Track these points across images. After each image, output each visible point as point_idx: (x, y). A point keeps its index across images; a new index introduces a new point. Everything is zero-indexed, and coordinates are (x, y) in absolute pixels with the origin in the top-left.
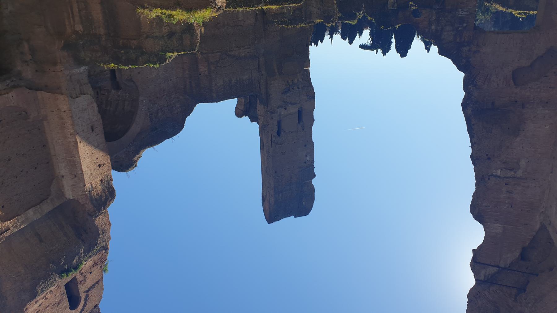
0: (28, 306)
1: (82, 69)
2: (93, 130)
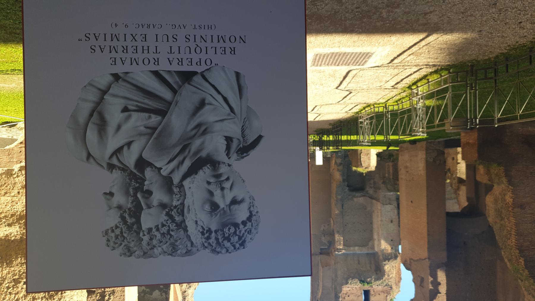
0: (344, 286)
1: (392, 193)
2: (392, 222)
